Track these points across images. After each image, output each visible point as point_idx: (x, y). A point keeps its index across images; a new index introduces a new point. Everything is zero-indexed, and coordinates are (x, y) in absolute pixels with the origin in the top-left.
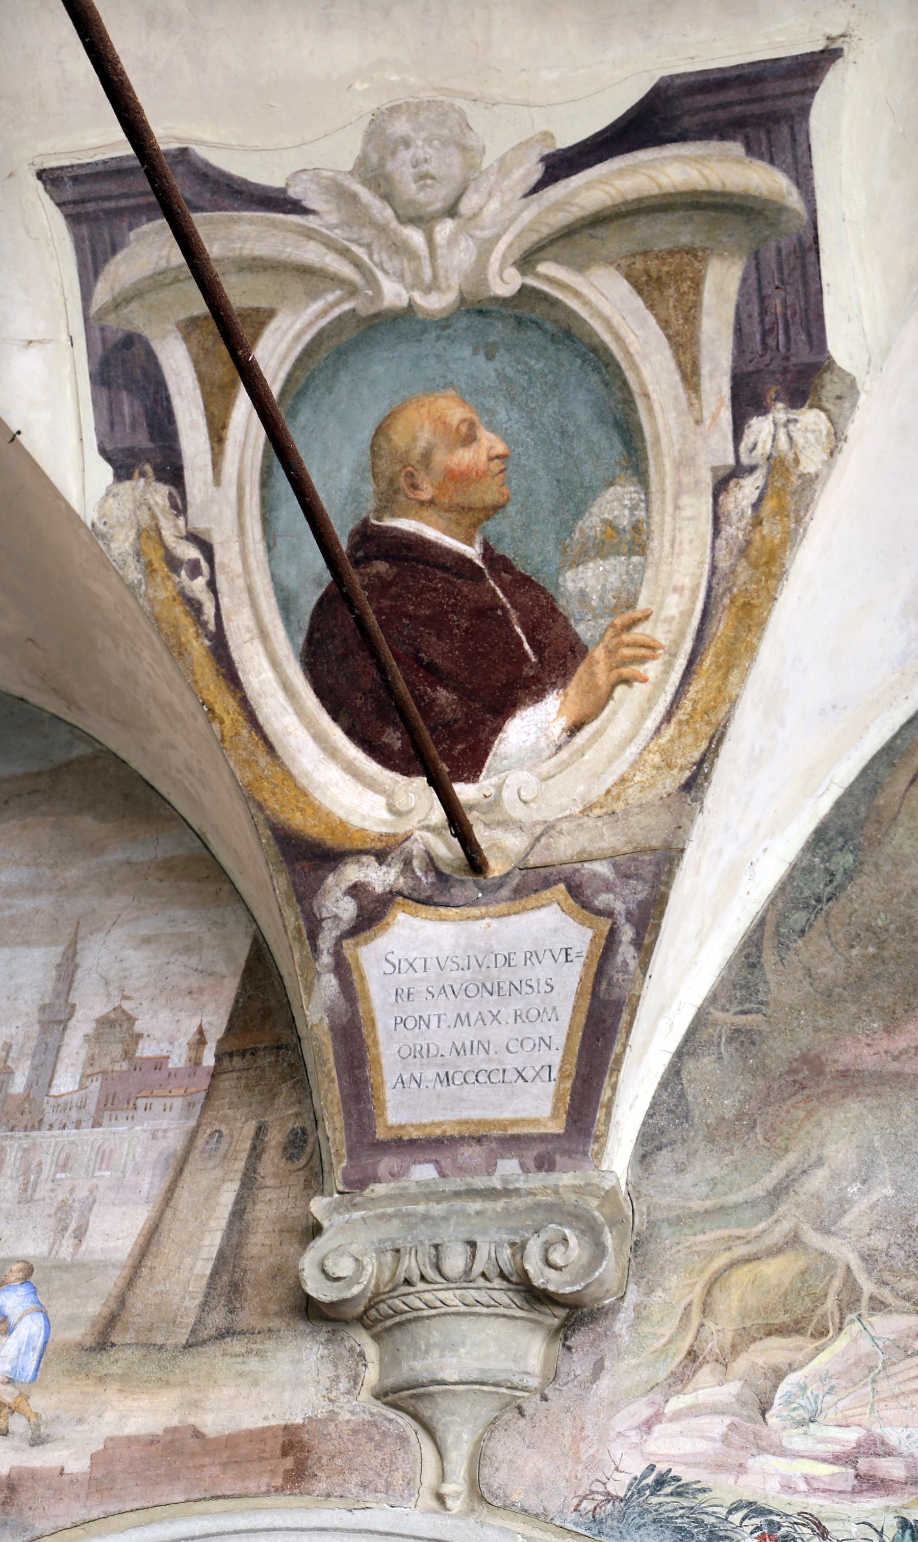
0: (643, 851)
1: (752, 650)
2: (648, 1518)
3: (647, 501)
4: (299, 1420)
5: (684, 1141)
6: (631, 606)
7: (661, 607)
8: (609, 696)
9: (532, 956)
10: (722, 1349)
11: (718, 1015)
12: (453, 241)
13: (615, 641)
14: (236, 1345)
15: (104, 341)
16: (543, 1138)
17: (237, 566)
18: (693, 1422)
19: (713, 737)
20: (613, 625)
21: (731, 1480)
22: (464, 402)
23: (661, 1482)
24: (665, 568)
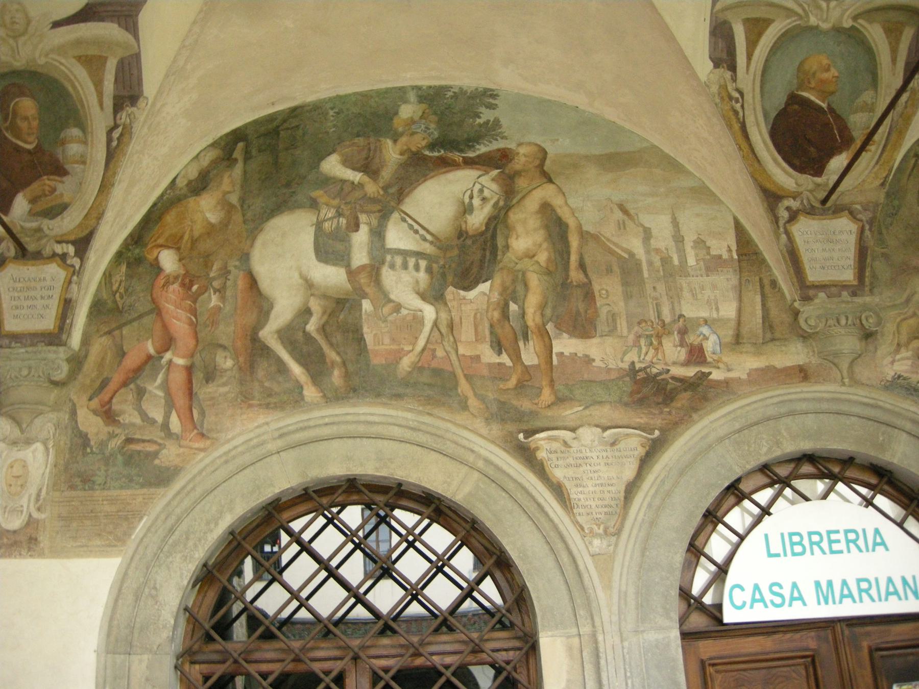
4: (801, 363)
9: (841, 232)
12: (835, 8)
14: (777, 343)
15: (716, 21)
16: (852, 286)
17: (751, 101)
22: (828, 58)
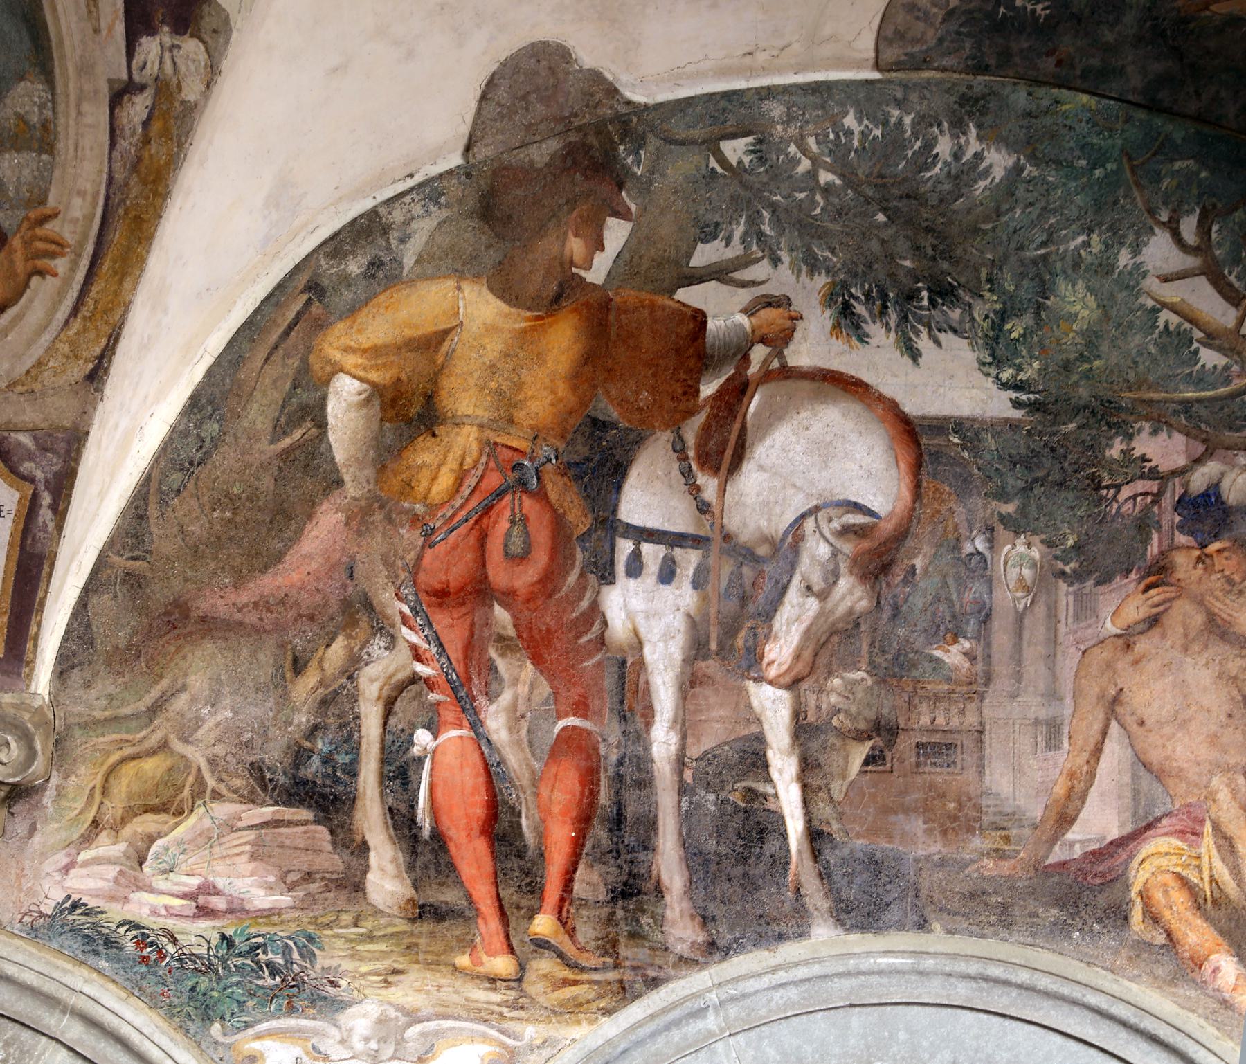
0: (57, 429)
1: (142, 261)
2: (67, 928)
3: (54, 101)
5: (90, 663)
6: (42, 202)
7: (68, 207)
8: (26, 285)
10: (115, 820)
11: (115, 559)
13: (30, 233)
18: (96, 869)
19: (110, 336)
20: (27, 218)
21: (119, 907)
23: (75, 906)
24: (70, 170)
